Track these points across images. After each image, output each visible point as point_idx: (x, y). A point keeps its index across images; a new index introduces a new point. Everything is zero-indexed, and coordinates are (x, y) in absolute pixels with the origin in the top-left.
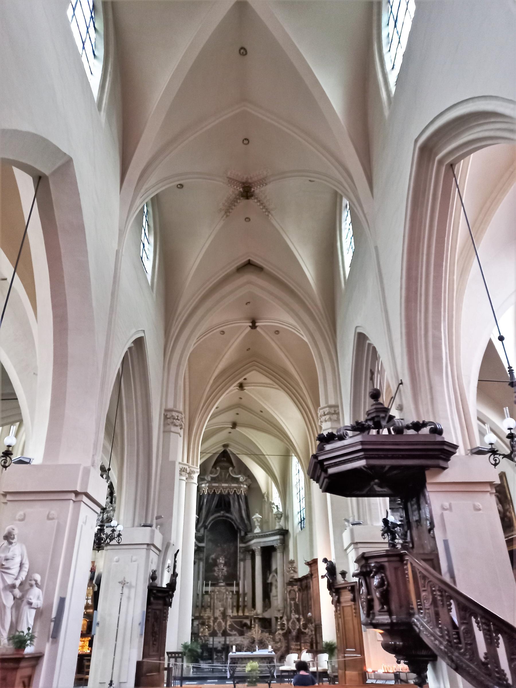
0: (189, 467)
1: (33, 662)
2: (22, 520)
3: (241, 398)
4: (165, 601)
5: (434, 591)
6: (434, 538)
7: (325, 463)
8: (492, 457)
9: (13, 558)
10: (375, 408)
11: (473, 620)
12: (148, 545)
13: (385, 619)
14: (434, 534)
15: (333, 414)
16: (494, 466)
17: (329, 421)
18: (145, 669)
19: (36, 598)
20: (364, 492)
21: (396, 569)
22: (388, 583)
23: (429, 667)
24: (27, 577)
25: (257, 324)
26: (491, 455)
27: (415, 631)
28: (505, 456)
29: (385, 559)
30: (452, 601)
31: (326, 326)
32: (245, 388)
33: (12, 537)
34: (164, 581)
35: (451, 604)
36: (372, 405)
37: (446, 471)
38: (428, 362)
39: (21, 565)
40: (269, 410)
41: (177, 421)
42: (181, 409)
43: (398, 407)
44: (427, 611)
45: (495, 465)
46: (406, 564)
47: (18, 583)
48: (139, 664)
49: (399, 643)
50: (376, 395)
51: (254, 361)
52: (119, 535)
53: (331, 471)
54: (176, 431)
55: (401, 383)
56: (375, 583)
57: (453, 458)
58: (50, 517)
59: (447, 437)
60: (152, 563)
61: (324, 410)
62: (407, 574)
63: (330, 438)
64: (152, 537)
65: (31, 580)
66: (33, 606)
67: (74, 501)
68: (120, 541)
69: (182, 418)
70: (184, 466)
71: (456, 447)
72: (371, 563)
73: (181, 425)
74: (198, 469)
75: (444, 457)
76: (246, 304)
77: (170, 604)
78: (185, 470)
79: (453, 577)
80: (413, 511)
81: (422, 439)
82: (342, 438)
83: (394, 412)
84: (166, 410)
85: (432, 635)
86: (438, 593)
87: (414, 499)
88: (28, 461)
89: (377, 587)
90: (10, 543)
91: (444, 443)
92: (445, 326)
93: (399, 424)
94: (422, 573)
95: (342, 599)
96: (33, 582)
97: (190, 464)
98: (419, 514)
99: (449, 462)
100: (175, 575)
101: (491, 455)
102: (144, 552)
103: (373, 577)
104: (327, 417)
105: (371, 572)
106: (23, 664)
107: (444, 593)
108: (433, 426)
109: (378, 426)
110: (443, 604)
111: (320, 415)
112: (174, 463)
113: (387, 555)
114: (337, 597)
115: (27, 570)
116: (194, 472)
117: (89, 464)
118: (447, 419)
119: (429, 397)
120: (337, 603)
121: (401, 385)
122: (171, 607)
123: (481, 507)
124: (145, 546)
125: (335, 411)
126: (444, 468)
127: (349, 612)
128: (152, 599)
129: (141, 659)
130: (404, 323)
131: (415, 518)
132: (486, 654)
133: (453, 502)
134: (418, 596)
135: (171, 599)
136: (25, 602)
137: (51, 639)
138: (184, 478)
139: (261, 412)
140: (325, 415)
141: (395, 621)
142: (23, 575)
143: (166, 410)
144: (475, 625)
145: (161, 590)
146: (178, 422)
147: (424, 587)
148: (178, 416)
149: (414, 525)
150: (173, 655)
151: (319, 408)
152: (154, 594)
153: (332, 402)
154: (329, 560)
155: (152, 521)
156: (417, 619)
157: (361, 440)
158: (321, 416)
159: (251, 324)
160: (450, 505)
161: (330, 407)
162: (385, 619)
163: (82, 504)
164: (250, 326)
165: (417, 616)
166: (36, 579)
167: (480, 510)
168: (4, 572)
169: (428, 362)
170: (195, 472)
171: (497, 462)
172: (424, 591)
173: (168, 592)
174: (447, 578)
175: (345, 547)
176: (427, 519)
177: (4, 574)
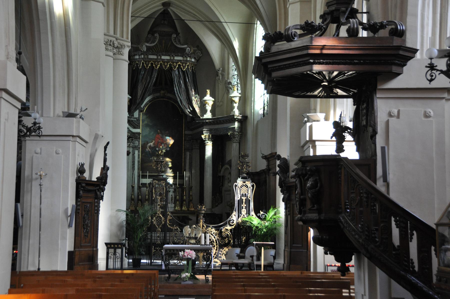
0: (117, 39)
4: (96, 194)
5: (362, 193)
6: (375, 144)
7: (269, 66)
8: (430, 72)
11: (393, 219)
12: (73, 136)
13: (314, 216)
16: (428, 82)
18: (77, 259)
28: (442, 72)
37: (401, 75)
44: (353, 210)
45: (431, 81)
46: (341, 169)
48: (70, 253)
56: (308, 185)
57: (410, 63)
60: (78, 155)
64: (78, 128)
71: (415, 51)
72: (307, 167)
75: (399, 62)
77: (102, 198)
78: (111, 44)
85: (354, 230)
86: (365, 195)
87: (365, 105)
89: (310, 188)
93: (354, 25)
94: (353, 177)
97: (118, 35)
99: (405, 68)
103: (308, 180)
105: (306, 175)
108: (393, 27)
114: (287, 195)
118: (416, 16)
122: (103, 201)
123: (432, 114)
124: (71, 138)
126: (399, 74)
128: (81, 192)
133: (401, 109)
135: (102, 193)
141: (322, 218)
144: (393, 223)
145: (90, 183)
147: (353, 190)
152: (83, 187)
154: (282, 157)
160: (399, 112)
162: (314, 216)
165: (343, 215)
167: (430, 117)
170: (124, 46)
171: (433, 78)
172: (352, 193)
173: (98, 185)
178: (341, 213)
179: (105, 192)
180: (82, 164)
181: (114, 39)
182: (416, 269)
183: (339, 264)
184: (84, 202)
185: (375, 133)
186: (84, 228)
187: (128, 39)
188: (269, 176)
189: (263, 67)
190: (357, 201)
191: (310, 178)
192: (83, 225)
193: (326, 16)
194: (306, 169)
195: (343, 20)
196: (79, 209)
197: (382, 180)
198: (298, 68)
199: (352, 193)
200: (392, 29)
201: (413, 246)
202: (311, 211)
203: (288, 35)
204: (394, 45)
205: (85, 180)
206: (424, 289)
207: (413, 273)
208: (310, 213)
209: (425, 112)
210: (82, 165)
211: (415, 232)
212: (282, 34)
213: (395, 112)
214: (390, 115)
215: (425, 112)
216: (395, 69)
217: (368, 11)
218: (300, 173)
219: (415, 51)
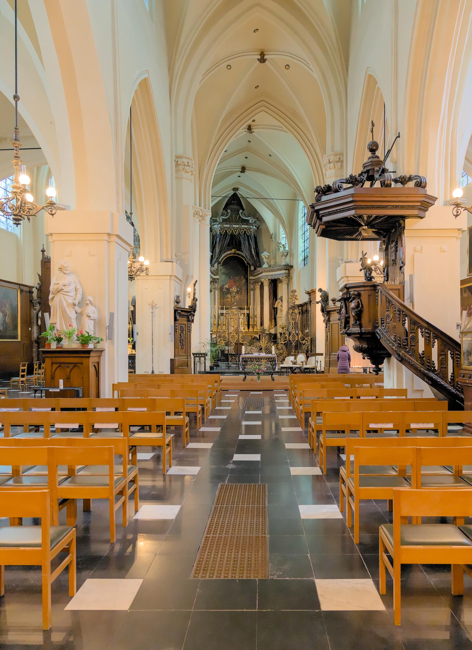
1: (99, 354)
5: (395, 311)
7: (320, 212)
11: (419, 330)
13: (356, 330)
21: (369, 296)
22: (362, 307)
23: (385, 361)
26: (455, 207)
27: (377, 337)
30: (406, 318)
35: (405, 320)
36: (369, 158)
42: (191, 156)
44: (387, 325)
46: (378, 293)
48: (172, 361)
49: (365, 346)
50: (373, 148)
53: (325, 219)
55: (399, 137)
57: (430, 209)
59: (430, 191)
63: (328, 190)
66: (91, 318)
68: (148, 273)
69: (192, 164)
70: (197, 210)
71: (435, 199)
72: (351, 291)
73: (192, 171)
77: (193, 321)
79: (412, 302)
81: (407, 192)
83: (389, 165)
84: (177, 157)
87: (394, 243)
95: (331, 319)
100: (195, 300)
101: (455, 207)
103: (351, 301)
105: (350, 298)
109: (371, 178)
110: (400, 320)
114: (328, 317)
120: (328, 321)
121: (398, 139)
128: (178, 317)
129: (173, 358)
131: (393, 258)
136: (85, 316)
138: (198, 221)
141: (363, 331)
143: (177, 157)
144: (420, 334)
148: (188, 163)
150: (198, 355)
152: (179, 313)
162: (357, 330)
165: (380, 328)
167: (445, 251)
173: (190, 312)
174: (407, 303)
175: (338, 280)
178: (378, 327)
179: (195, 317)
180: (178, 297)
183: (374, 366)
186: (181, 342)
188: (311, 306)
189: (315, 213)
190: (391, 317)
191: (353, 300)
192: (180, 340)
193: (364, 174)
194: (350, 294)
195: (376, 176)
196: (177, 329)
199: (388, 311)
201: (435, 351)
207: (434, 371)
210: (178, 297)
211: (436, 340)
212: (330, 187)
219: (434, 199)
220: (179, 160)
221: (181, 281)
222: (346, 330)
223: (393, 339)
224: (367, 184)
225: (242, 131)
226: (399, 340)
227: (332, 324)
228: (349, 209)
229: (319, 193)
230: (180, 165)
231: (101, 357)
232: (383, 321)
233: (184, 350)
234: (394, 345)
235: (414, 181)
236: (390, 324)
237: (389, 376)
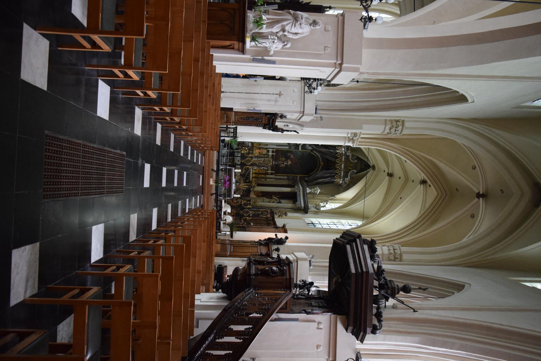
0: (357, 139)
1: (241, 49)
2: (325, 30)
3: (413, 181)
4: (267, 125)
5: (268, 305)
6: (300, 313)
7: (354, 243)
9: (301, 28)
10: (395, 287)
11: (251, 326)
12: (303, 112)
13: (253, 271)
14: (302, 313)
15: (395, 257)
17: (389, 252)
18: (229, 113)
19: (276, 46)
20: (332, 270)
22: (273, 277)
23: (225, 295)
24: (289, 38)
25: (481, 199)
29: (288, 277)
30: (262, 315)
31: (475, 260)
32: (422, 186)
33: (315, 26)
34: (279, 124)
35: (260, 314)
37: (345, 331)
38: (431, 334)
39: (296, 34)
40: (402, 204)
41: (394, 130)
42: (403, 133)
43: (395, 305)
47: (286, 33)
48: (231, 109)
50: (406, 289)
51: (446, 194)
52: (311, 92)
53: (348, 247)
54: (386, 130)
56: (274, 268)
57: (354, 337)
58: (326, 48)
59: (369, 337)
60: (292, 115)
61: (399, 249)
62: (278, 290)
63: (373, 250)
64: (308, 115)
65: (287, 41)
67: (336, 63)
69: (396, 134)
71: (362, 341)
72: (286, 267)
73: (391, 134)
74: (356, 146)
76: (501, 190)
77: (264, 128)
78: (355, 136)
79: (276, 320)
80: (318, 303)
81: (369, 318)
82: (372, 258)
83: (391, 302)
84: (403, 121)
85: (243, 299)
87: (326, 305)
88: (366, 27)
89: (271, 269)
90: (310, 25)
91: (365, 333)
92: (462, 354)
93: (381, 302)
95: (262, 247)
96: (286, 43)
97: (360, 140)
98: (316, 306)
100: (282, 131)
102: (299, 110)
103: (277, 267)
104: (392, 251)
106: (241, 44)
107: (267, 311)
108: (378, 328)
110: (260, 309)
111: (394, 246)
112: (361, 128)
113: (290, 279)
114: (263, 243)
115: (293, 38)
116: (353, 143)
117: (361, 71)
118: (384, 340)
119: (402, 330)
123: (319, 350)
124: (302, 110)
125: (397, 258)
126: (347, 330)
127: (254, 250)
128: (269, 116)
129: (234, 110)
130: (468, 321)
131: (313, 303)
132: (232, 329)
133: (323, 331)
134: (266, 295)
137: (252, 57)
138: (349, 135)
139: (401, 198)
140: (394, 250)
141: (251, 277)
142: (290, 36)
143: (403, 121)
144: (248, 327)
145: (274, 121)
146: (393, 130)
147: (270, 299)
148: (398, 131)
149: (309, 302)
151: (400, 246)
152: (272, 117)
153: (405, 257)
154: (287, 240)
155: (320, 114)
156: (252, 291)
157: (370, 272)
158: (393, 246)
159: (481, 193)
160: (321, 329)
161: (401, 255)
162: (253, 271)
163: (334, 69)
164: (479, 192)
166: (288, 44)
167: (317, 349)
168: (293, 23)
169: (431, 334)
170: (353, 143)
172: (268, 298)
174: (274, 316)
175: (295, 253)
176: (312, 310)
177: (291, 23)
178: (255, 290)
179: (268, 130)
181: (358, 138)
182: (217, 340)
184: (262, 118)
185: (308, 313)
186: (246, 117)
187: (358, 145)
189: (353, 239)
190: (263, 302)
191: (278, 269)
194: (284, 266)
195: (382, 292)
196: (258, 114)
197: (277, 317)
198: (353, 264)
200: (377, 326)
201: (233, 339)
202: (257, 269)
203: (375, 257)
204: (367, 328)
205: (276, 119)
206: (204, 345)
208: (255, 268)
209: (320, 346)
211: (241, 341)
213: (321, 326)
214: (319, 323)
215: (320, 346)
216: (350, 328)
217: (386, 306)
218: (282, 262)
220: (401, 123)
221: (299, 120)
222: (253, 262)
223: (244, 303)
224: (376, 283)
225: (423, 176)
226: (243, 308)
227: (257, 247)
228: (356, 268)
229: (370, 242)
230: (397, 124)
231: (238, 51)
232: (260, 295)
233: (240, 120)
234: (239, 303)
235: (377, 324)
236: (257, 300)
237: (211, 298)
